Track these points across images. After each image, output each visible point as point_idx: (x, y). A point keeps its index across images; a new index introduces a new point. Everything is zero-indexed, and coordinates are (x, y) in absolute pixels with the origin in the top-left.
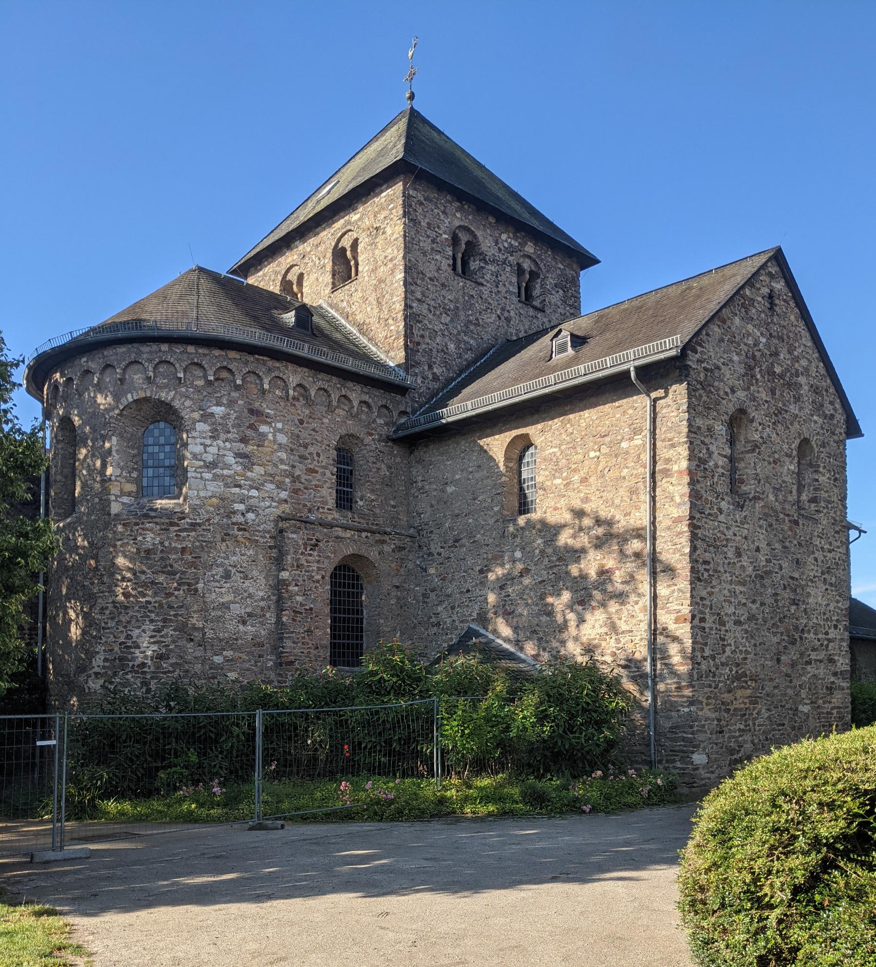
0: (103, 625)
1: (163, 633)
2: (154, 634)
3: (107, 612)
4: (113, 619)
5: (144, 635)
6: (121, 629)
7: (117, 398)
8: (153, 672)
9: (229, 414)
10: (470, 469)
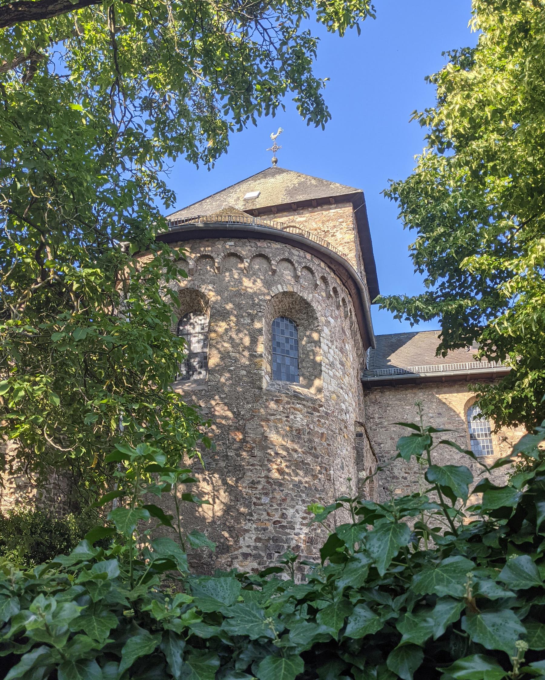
0: (254, 500)
2: (305, 515)
3: (260, 487)
4: (266, 494)
5: (297, 515)
6: (276, 507)
7: (268, 284)
10: (431, 415)
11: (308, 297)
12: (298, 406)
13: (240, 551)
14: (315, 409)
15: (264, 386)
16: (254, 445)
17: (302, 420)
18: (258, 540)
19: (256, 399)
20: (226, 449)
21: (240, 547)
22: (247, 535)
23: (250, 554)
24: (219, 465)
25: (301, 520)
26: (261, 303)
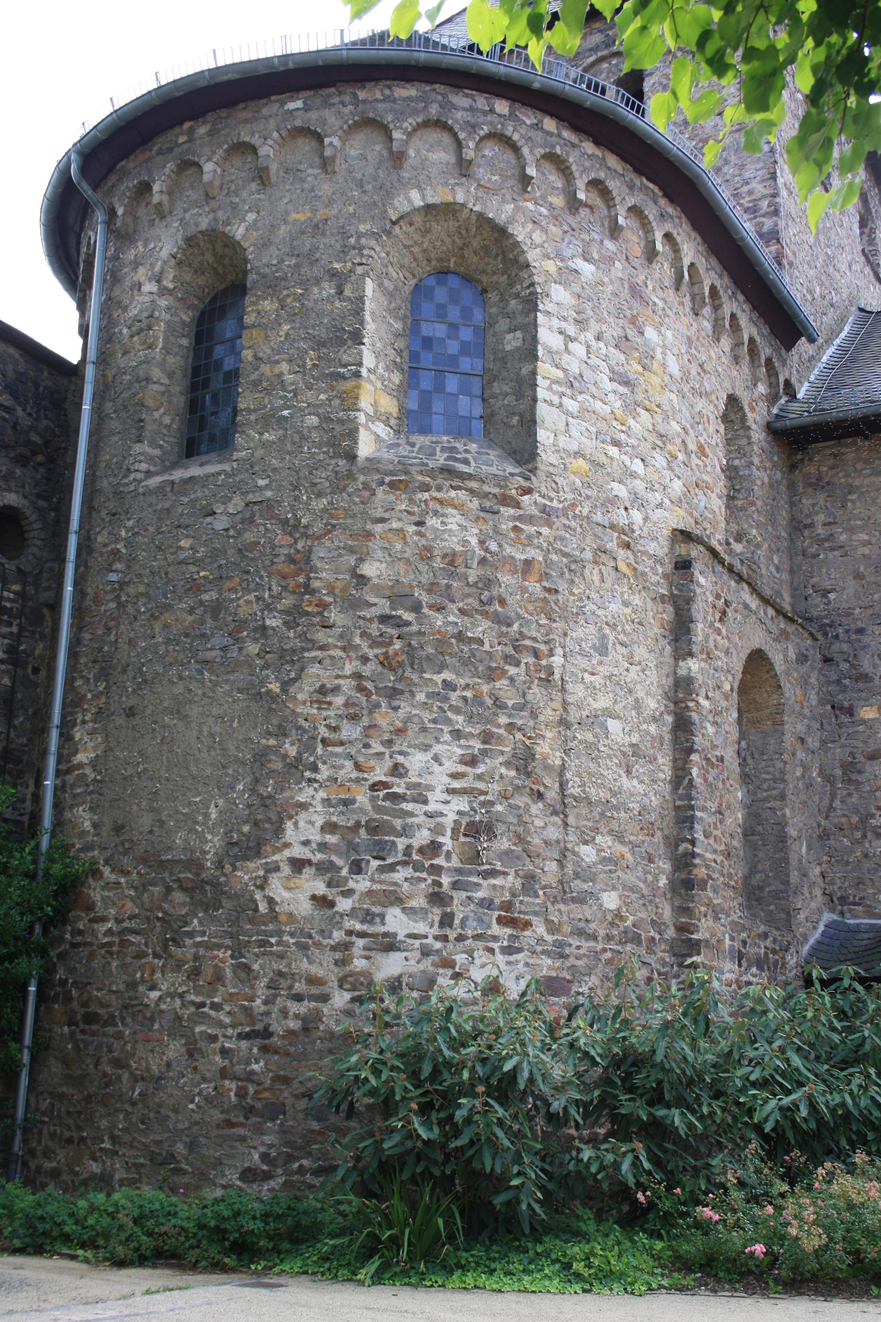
0: (323, 732)
1: (481, 769)
2: (461, 768)
3: (339, 700)
4: (354, 718)
5: (436, 768)
6: (377, 747)
8: (459, 871)
9: (601, 283)
11: (501, 210)
12: (453, 493)
13: (287, 853)
14: (506, 500)
15: (365, 448)
16: (329, 599)
17: (463, 528)
18: (329, 827)
19: (340, 483)
20: (262, 611)
21: (287, 845)
22: (303, 817)
23: (309, 862)
24: (245, 652)
25: (447, 780)
26: (363, 241)
